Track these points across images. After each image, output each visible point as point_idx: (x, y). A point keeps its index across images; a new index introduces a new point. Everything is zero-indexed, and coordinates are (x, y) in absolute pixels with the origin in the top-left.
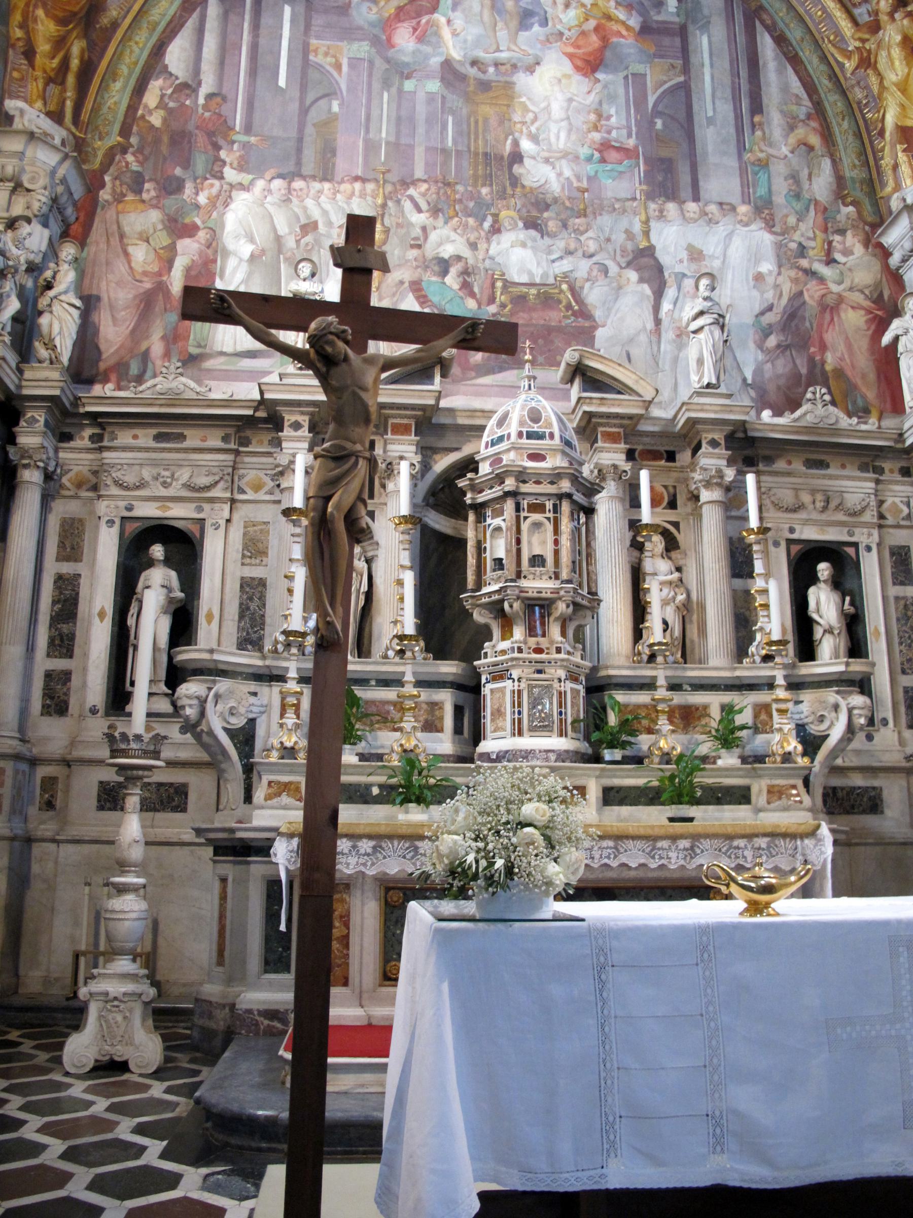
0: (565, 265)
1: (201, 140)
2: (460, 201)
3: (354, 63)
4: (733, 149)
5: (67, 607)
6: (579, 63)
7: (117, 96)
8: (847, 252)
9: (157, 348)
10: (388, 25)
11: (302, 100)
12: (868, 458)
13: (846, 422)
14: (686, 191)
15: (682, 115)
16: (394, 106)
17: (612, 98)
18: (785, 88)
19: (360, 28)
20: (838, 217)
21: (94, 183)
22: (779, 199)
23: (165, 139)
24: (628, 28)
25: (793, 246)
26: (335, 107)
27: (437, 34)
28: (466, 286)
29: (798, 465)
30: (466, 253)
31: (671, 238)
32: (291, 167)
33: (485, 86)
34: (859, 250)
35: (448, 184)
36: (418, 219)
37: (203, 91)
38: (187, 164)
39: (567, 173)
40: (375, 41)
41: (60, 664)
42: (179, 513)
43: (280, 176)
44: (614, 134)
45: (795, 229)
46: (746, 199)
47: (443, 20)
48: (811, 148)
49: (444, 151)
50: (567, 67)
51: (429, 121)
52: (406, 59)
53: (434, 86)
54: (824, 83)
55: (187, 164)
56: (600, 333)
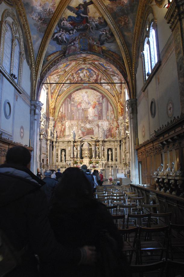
0: (91, 126)
1: (63, 117)
3: (75, 109)
5: (57, 155)
7: (56, 114)
8: (114, 123)
9: (62, 135)
10: (77, 105)
12: (114, 141)
13: (112, 139)
14: (101, 119)
18: (110, 108)
21: (56, 122)
22: (109, 119)
26: (74, 113)
28: (84, 129)
29: (108, 142)
30: (84, 126)
31: (100, 123)
33: (85, 111)
34: (116, 123)
36: (80, 123)
37: (63, 113)
40: (77, 107)
41: (57, 159)
42: (64, 148)
46: (106, 119)
48: (112, 114)
50: (92, 108)
53: (81, 111)
54: (114, 107)
56: (94, 132)
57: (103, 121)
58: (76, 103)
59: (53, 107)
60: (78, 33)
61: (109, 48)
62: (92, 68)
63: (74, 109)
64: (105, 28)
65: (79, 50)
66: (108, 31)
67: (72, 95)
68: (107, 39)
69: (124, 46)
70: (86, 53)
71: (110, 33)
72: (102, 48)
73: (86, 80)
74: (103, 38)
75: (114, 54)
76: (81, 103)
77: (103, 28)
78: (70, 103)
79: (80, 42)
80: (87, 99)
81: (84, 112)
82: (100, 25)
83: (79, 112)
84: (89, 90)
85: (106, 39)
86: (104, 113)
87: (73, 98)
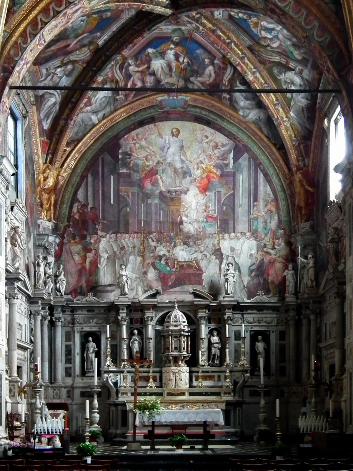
2: (165, 238)
4: (246, 214)
6: (201, 189)
11: (118, 208)
14: (231, 230)
15: (232, 205)
16: (145, 208)
17: (210, 200)
19: (135, 182)
20: (278, 234)
22: (260, 230)
23: (80, 222)
24: (216, 175)
25: (263, 244)
26: (128, 210)
27: (157, 182)
31: (225, 245)
32: (116, 230)
33: (172, 199)
35: (161, 233)
38: (87, 230)
39: (196, 226)
43: (114, 233)
44: (210, 213)
45: (263, 239)
47: (159, 177)
48: (271, 212)
49: (161, 222)
50: (197, 191)
51: (156, 213)
52: (148, 192)
53: (157, 201)
55: (87, 230)
57: (238, 239)
58: (138, 172)
59: (51, 182)
62: (198, 37)
63: (129, 192)
67: (122, 141)
73: (174, 85)
76: (156, 173)
78: (114, 171)
80: (177, 158)
81: (168, 205)
83: (148, 206)
84: (188, 124)
86: (241, 211)
87: (125, 154)
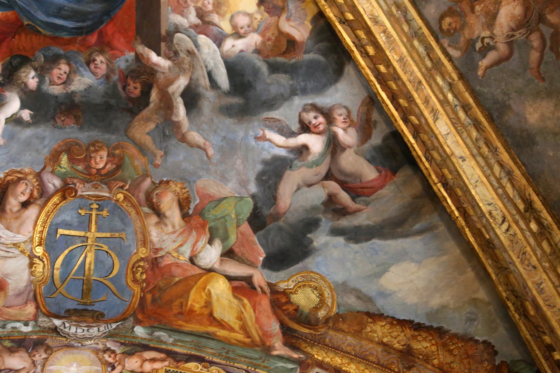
60: (44, 131)
61: (369, 289)
64: (325, 100)
65: (31, 309)
66: (350, 122)
68: (344, 197)
69: (534, 226)
70: (110, 336)
71: (376, 139)
72: (279, 300)
74: (296, 195)
75: (422, 345)
77: (304, 92)
79: (52, 244)
82: (274, 68)
85: (331, 199)
